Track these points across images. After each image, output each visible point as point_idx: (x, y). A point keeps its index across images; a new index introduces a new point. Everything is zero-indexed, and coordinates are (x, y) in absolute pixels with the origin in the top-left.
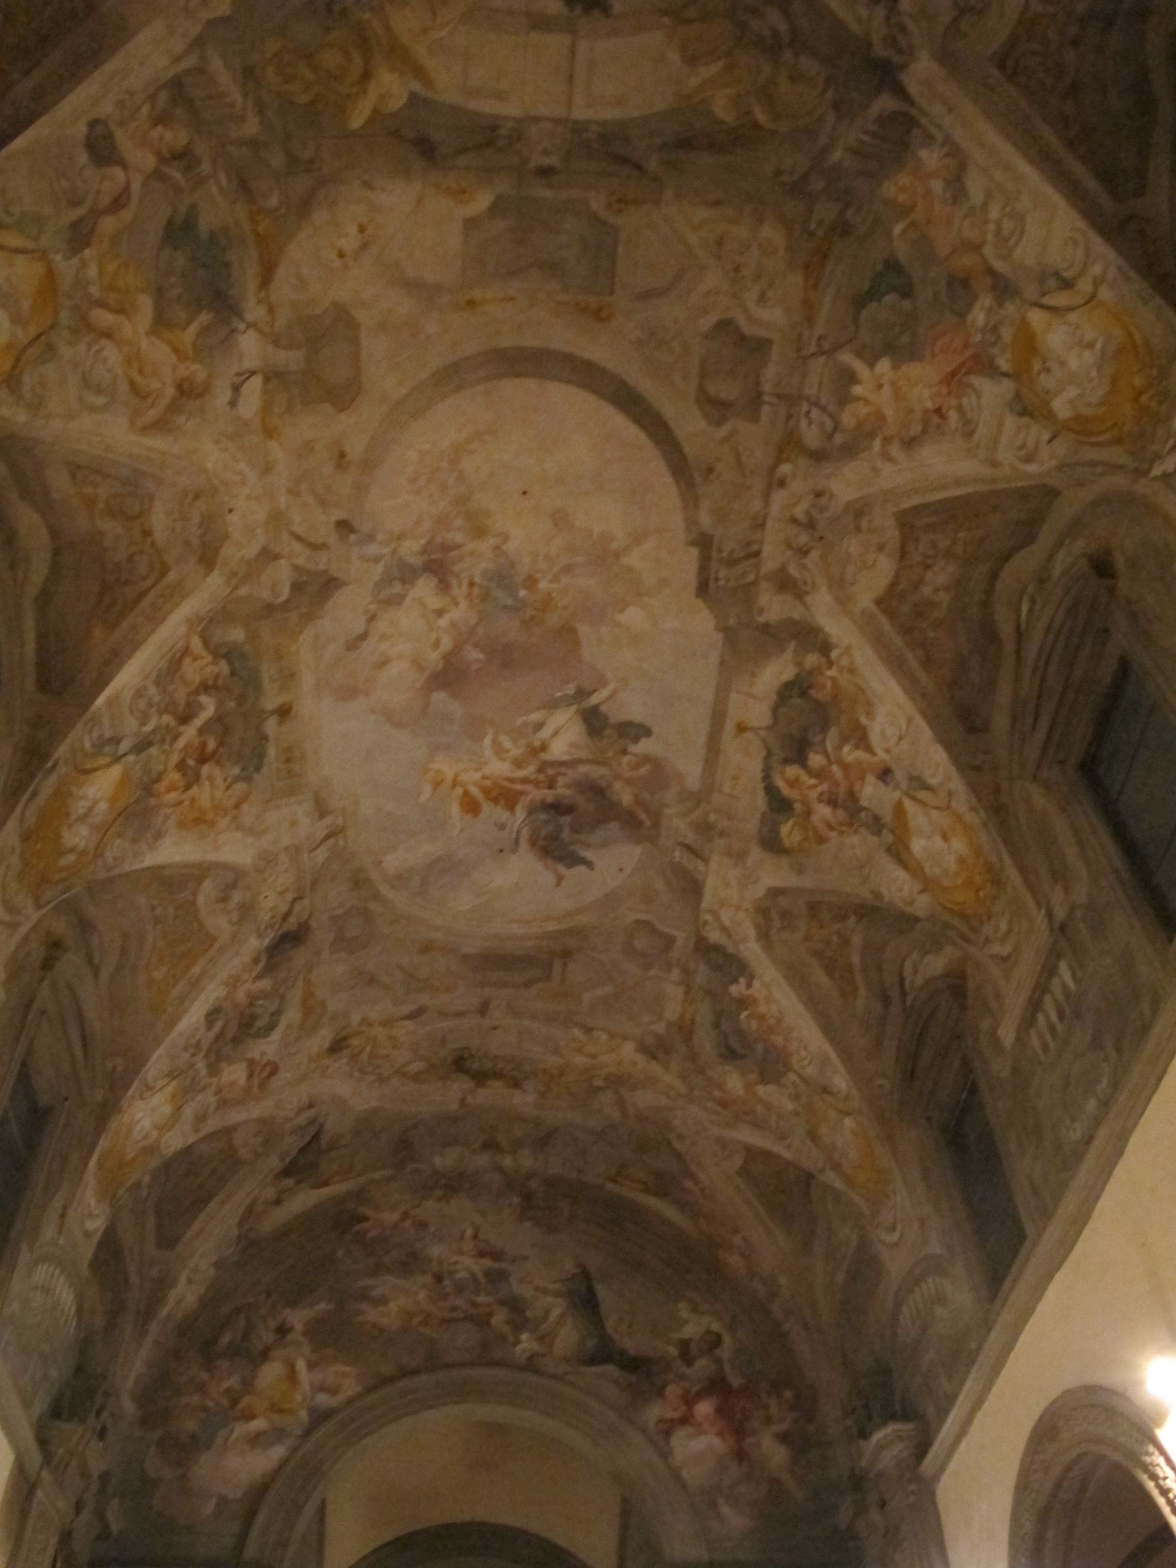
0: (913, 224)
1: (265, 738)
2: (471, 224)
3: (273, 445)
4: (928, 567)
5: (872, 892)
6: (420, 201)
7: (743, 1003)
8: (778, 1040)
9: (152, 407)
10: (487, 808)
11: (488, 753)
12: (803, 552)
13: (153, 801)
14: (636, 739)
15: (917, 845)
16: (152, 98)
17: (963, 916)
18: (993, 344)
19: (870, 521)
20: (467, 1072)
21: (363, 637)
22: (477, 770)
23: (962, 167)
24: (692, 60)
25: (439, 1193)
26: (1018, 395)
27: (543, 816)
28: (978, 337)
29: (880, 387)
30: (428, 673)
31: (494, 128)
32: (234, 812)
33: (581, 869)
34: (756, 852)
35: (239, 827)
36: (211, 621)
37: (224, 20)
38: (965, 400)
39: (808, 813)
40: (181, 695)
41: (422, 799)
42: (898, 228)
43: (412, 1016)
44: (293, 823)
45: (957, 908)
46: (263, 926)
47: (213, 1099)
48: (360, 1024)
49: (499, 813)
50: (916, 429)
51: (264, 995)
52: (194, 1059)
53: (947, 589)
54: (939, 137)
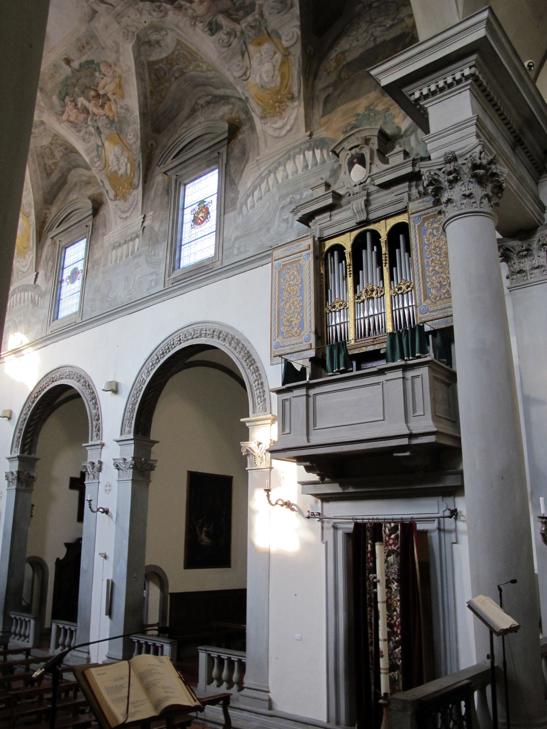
1: (80, 64)
13: (116, 119)
32: (113, 66)
35: (118, 60)
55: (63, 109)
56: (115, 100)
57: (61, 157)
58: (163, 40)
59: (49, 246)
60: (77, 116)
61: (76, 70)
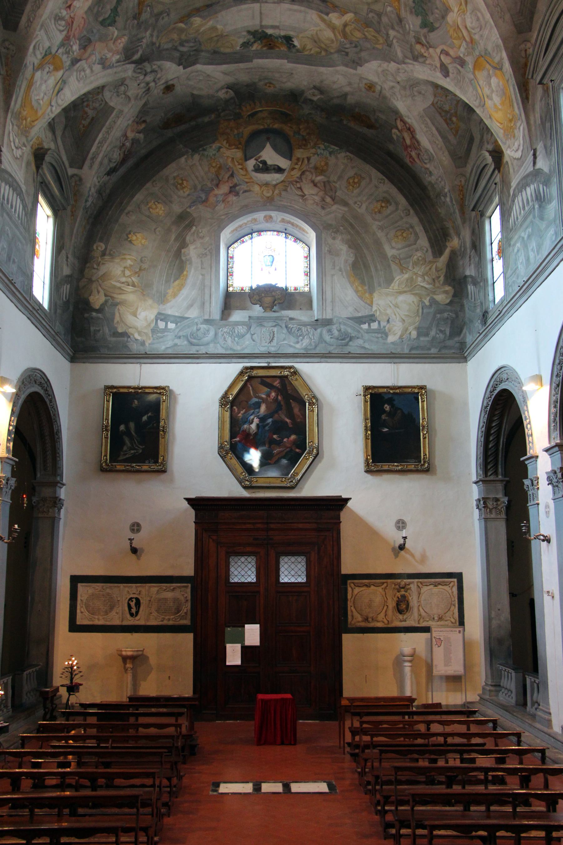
16: (424, 62)
24: (214, 28)
37: (395, 62)
38: (63, 23)
59: (541, 100)
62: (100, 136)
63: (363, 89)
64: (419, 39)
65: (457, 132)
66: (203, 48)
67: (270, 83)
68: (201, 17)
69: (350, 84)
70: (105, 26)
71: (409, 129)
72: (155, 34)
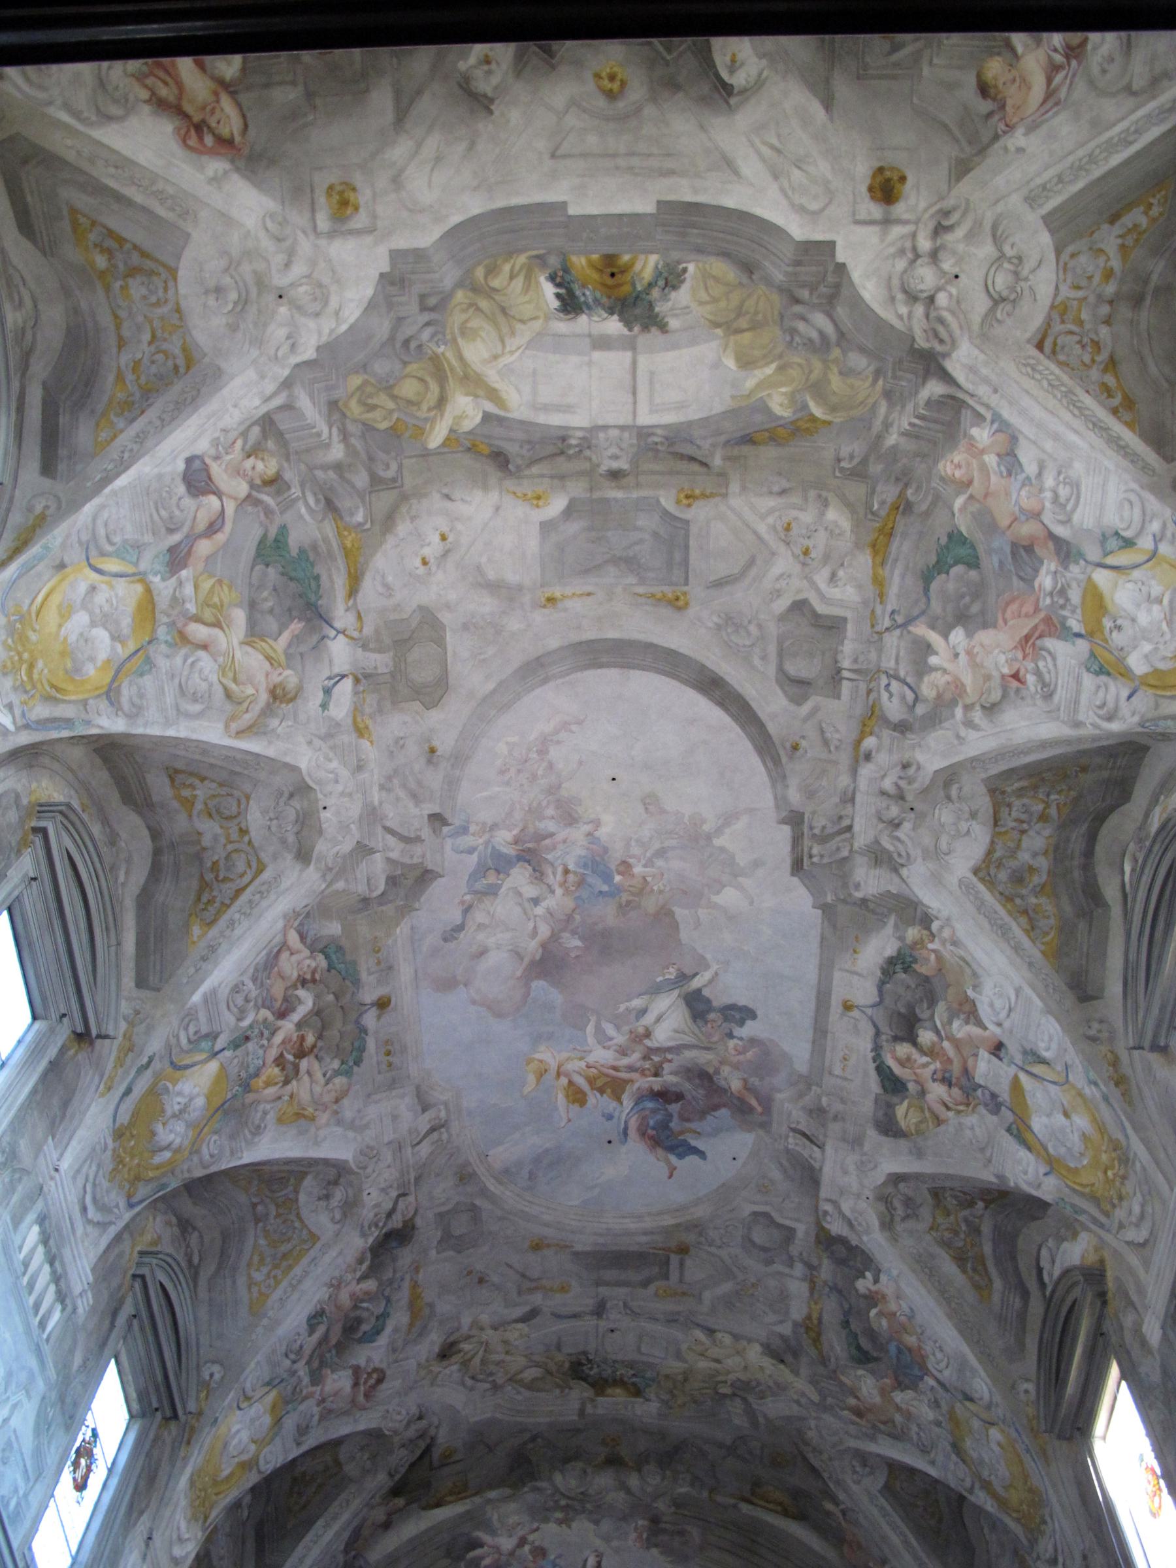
0: (971, 497)
1: (364, 1031)
2: (546, 527)
3: (365, 744)
4: (1023, 832)
5: (997, 1176)
6: (497, 509)
7: (873, 1299)
8: (911, 1340)
9: (247, 711)
10: (593, 1098)
11: (591, 1040)
12: (896, 825)
13: (250, 1097)
14: (741, 1023)
15: (1038, 1124)
16: (244, 434)
17: (1095, 1199)
18: (1063, 607)
19: (960, 789)
20: (584, 1379)
21: (460, 928)
22: (581, 1059)
23: (1014, 439)
24: (746, 362)
25: (559, 1515)
26: (1093, 655)
27: (650, 1105)
28: (1048, 601)
29: (956, 655)
30: (527, 960)
31: (564, 439)
33: (692, 1159)
34: (872, 1133)
35: (339, 1123)
36: (308, 915)
39: (923, 1093)
40: (278, 990)
41: (527, 1090)
42: (959, 502)
43: (525, 1319)
44: (395, 1118)
45: (1087, 1190)
46: (366, 1224)
47: (316, 1410)
48: (471, 1328)
49: (606, 1103)
50: (996, 696)
51: (369, 1297)
52: (296, 1366)
53: (1045, 853)
54: (989, 416)
55: (308, 941)
56: (280, 1098)
57: (199, 834)
58: (327, 1208)
60: (283, 978)
61: (361, 1015)
62: (1116, 160)
63: (358, 179)
64: (279, 493)
65: (75, 225)
66: (775, 297)
67: (611, 95)
68: (767, 410)
69: (397, 181)
70: (973, 547)
71: (199, 128)
72: (878, 424)
